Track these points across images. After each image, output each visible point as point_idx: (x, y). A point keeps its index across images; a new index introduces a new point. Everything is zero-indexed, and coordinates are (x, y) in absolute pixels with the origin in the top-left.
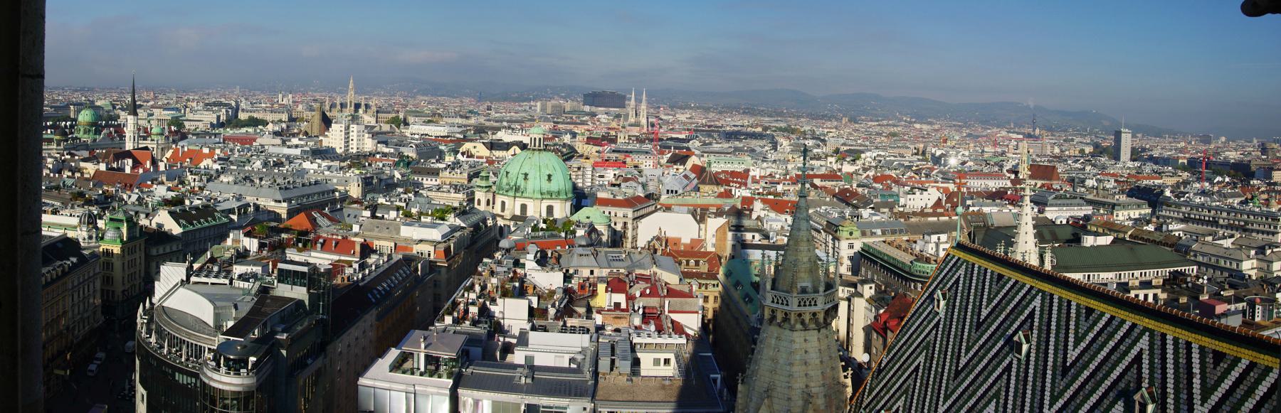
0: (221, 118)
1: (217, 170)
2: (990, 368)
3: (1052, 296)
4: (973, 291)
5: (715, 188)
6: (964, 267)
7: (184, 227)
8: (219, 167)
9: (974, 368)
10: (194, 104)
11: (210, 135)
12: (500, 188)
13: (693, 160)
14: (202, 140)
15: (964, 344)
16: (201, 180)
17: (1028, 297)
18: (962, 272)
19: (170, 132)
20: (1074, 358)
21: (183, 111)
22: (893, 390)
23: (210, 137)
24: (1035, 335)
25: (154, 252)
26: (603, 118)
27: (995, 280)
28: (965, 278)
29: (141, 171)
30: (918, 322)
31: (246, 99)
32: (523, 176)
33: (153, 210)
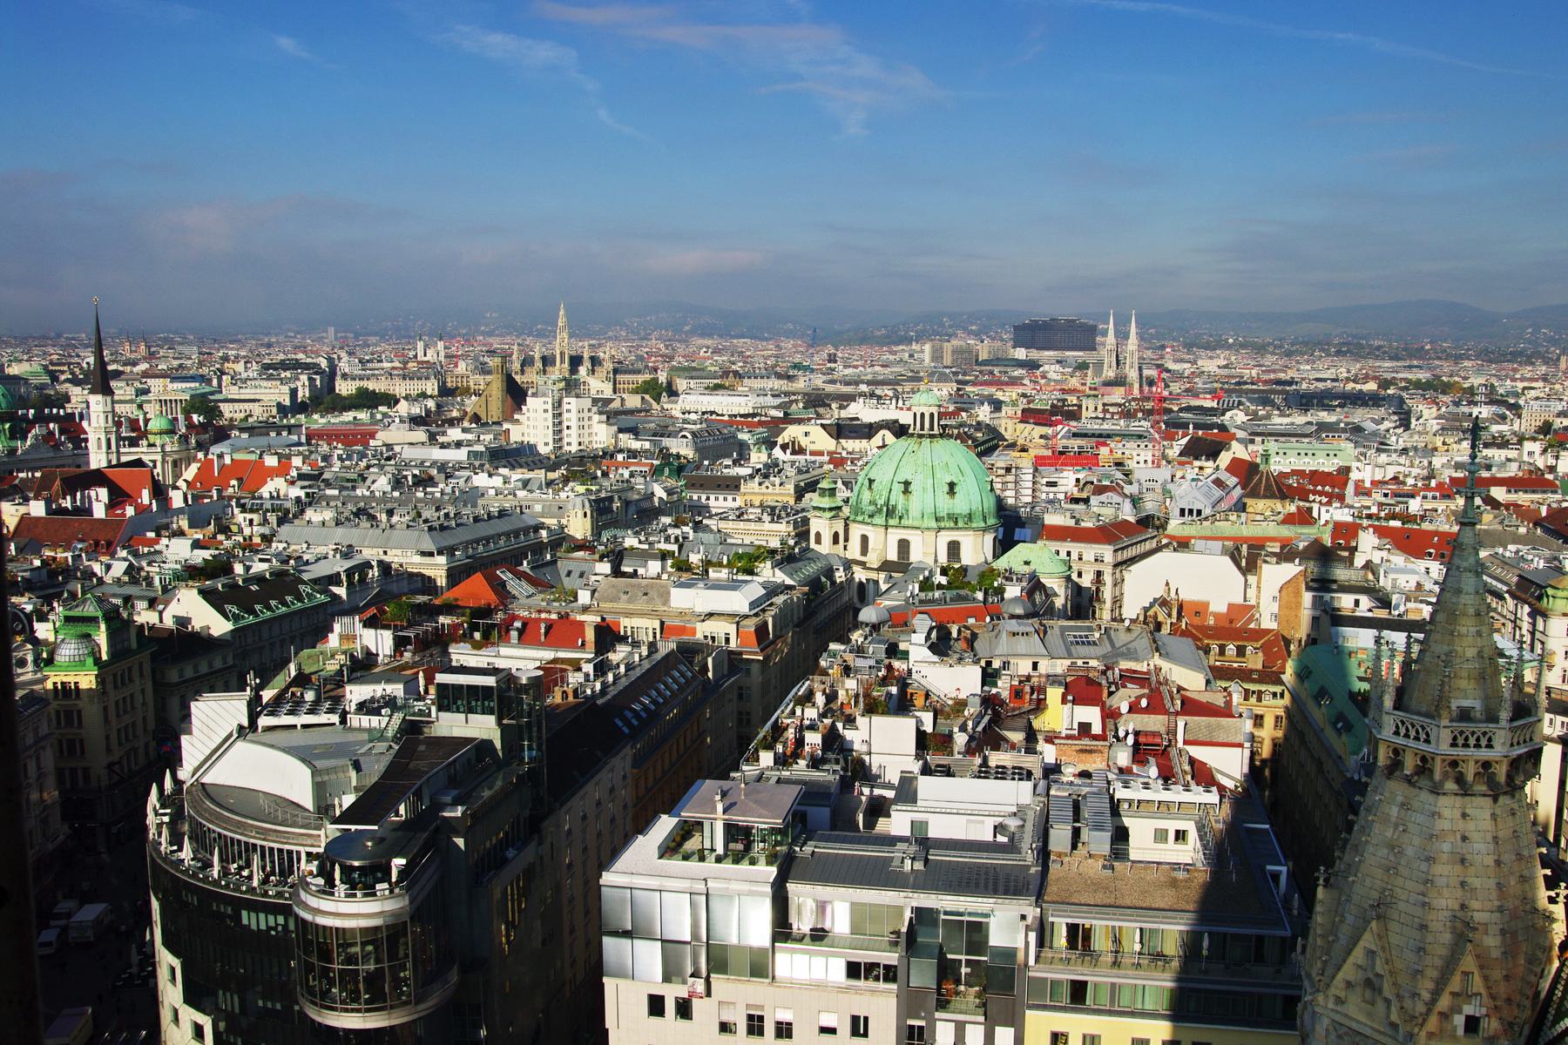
0: (300, 394)
1: (298, 499)
5: (1278, 506)
7: (236, 618)
8: (302, 494)
10: (240, 367)
11: (279, 429)
12: (857, 510)
13: (1238, 451)
14: (263, 441)
16: (265, 522)
19: (190, 426)
21: (215, 382)
23: (279, 434)
25: (173, 676)
26: (1053, 371)
29: (130, 511)
31: (350, 354)
32: (902, 487)
33: (165, 590)
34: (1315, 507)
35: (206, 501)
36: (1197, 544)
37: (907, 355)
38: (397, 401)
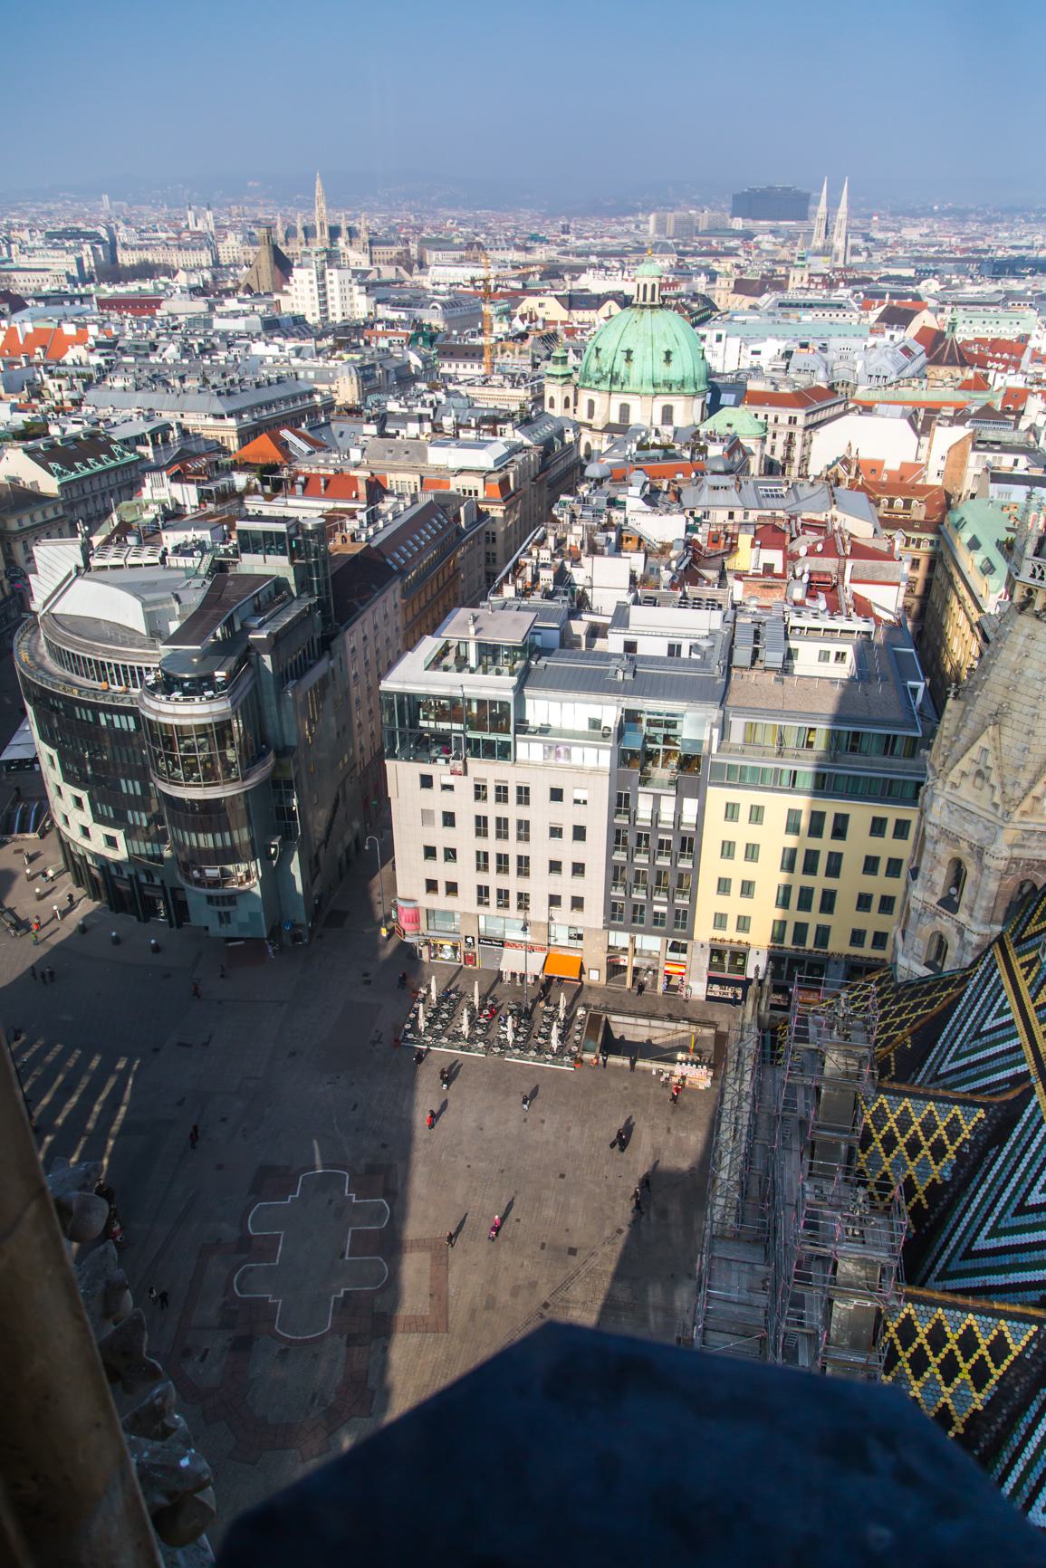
0: (86, 264)
1: (99, 367)
5: (957, 372)
7: (61, 474)
8: (102, 361)
11: (72, 299)
12: (585, 377)
13: (925, 319)
16: (72, 388)
23: (72, 303)
26: (766, 241)
31: (127, 223)
34: (992, 373)
35: (16, 367)
36: (880, 408)
38: (176, 272)
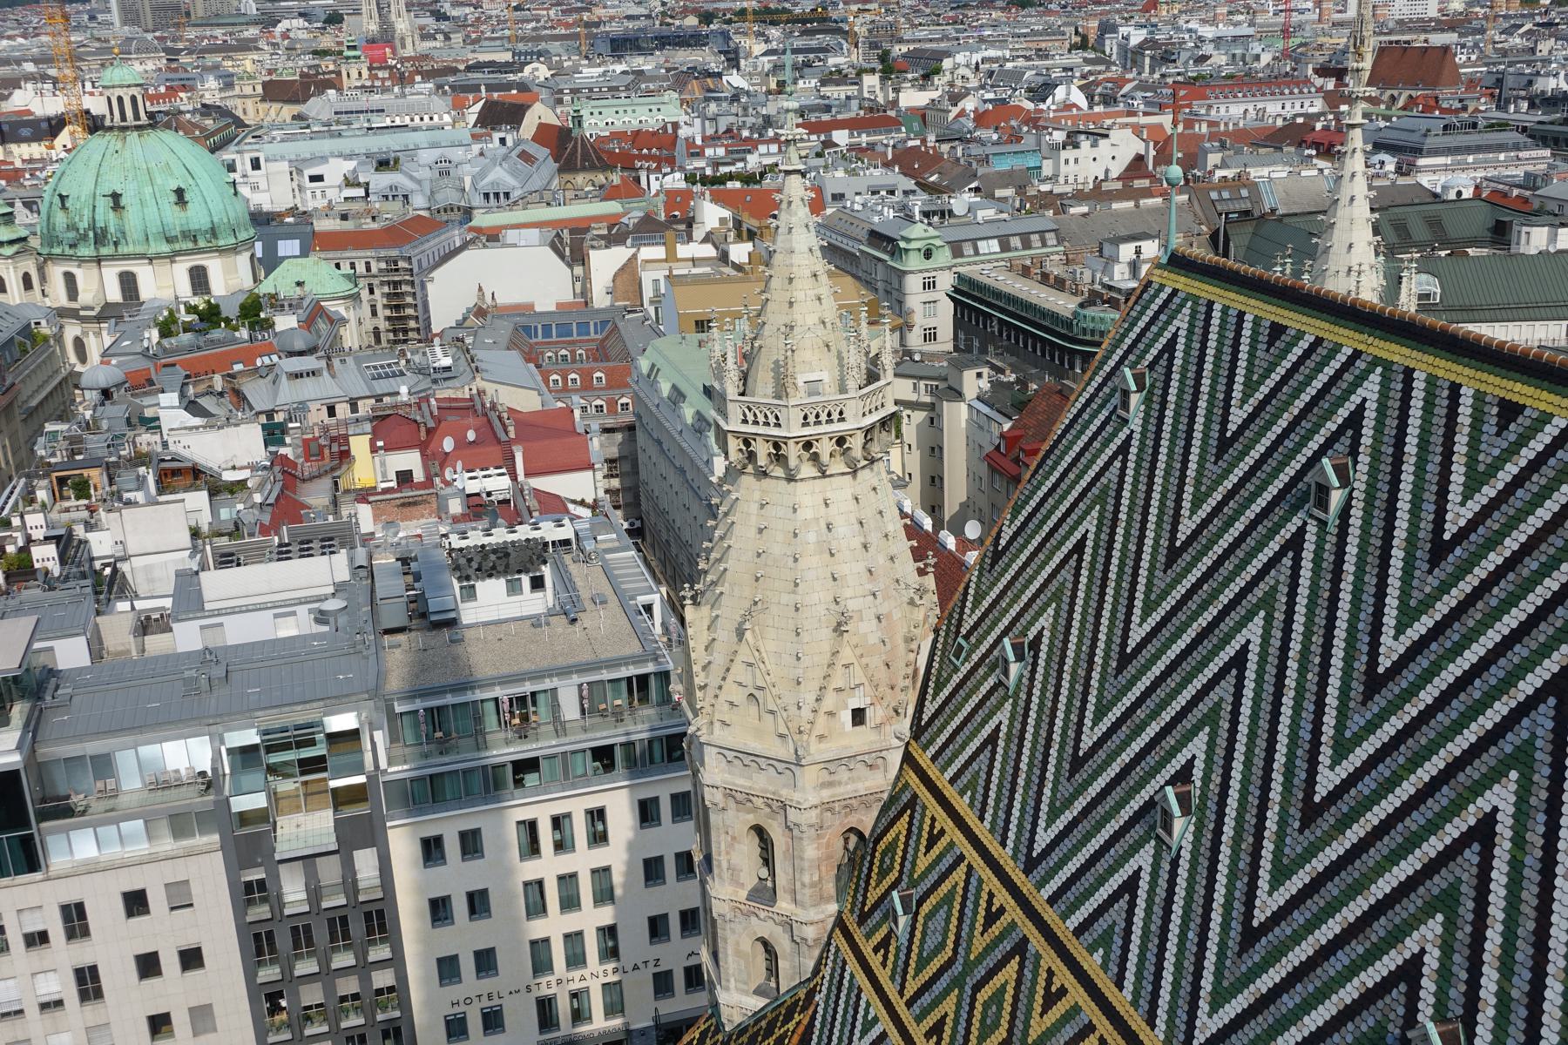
2: (1251, 542)
3: (1408, 373)
4: (1208, 366)
6: (1186, 311)
9: (1213, 542)
12: (51, 239)
13: (539, 114)
15: (1189, 489)
17: (1348, 377)
18: (1181, 322)
20: (1462, 522)
22: (1029, 594)
24: (1363, 467)
27: (1263, 338)
28: (1189, 339)
30: (1080, 444)
36: (511, 236)
37: (86, 17)
